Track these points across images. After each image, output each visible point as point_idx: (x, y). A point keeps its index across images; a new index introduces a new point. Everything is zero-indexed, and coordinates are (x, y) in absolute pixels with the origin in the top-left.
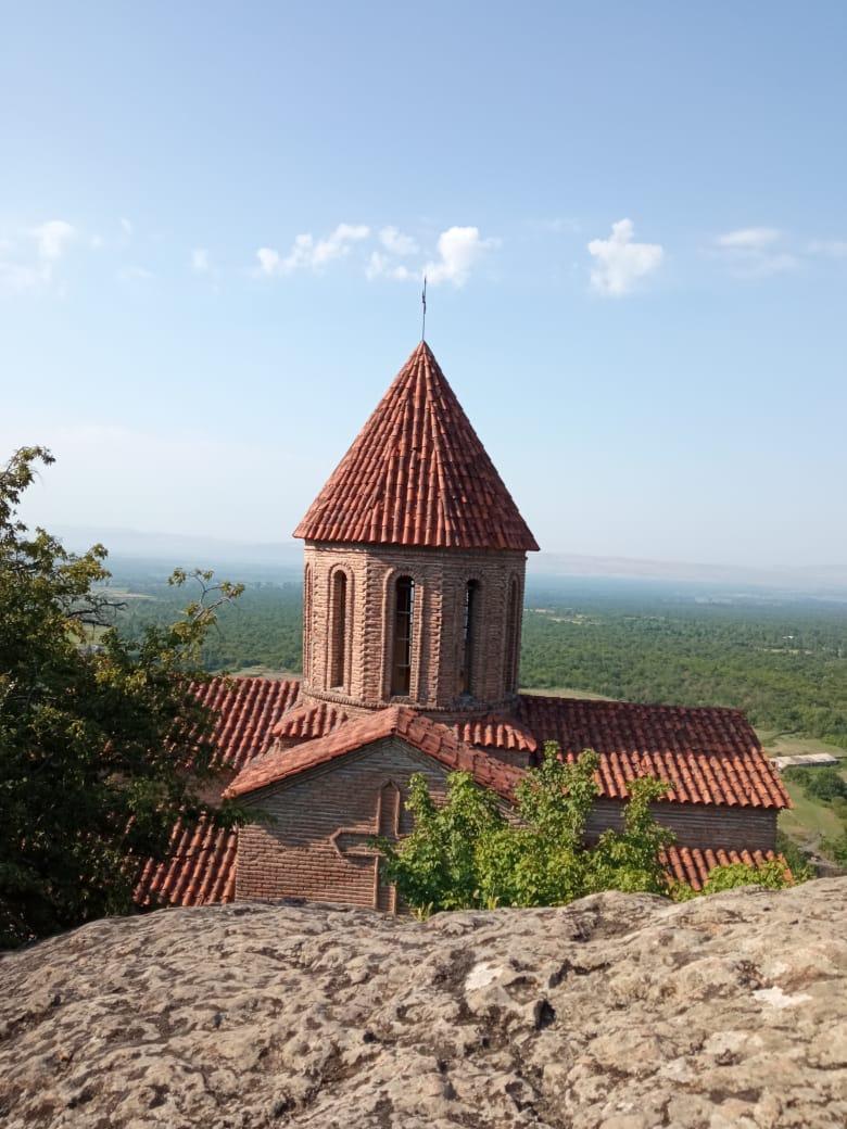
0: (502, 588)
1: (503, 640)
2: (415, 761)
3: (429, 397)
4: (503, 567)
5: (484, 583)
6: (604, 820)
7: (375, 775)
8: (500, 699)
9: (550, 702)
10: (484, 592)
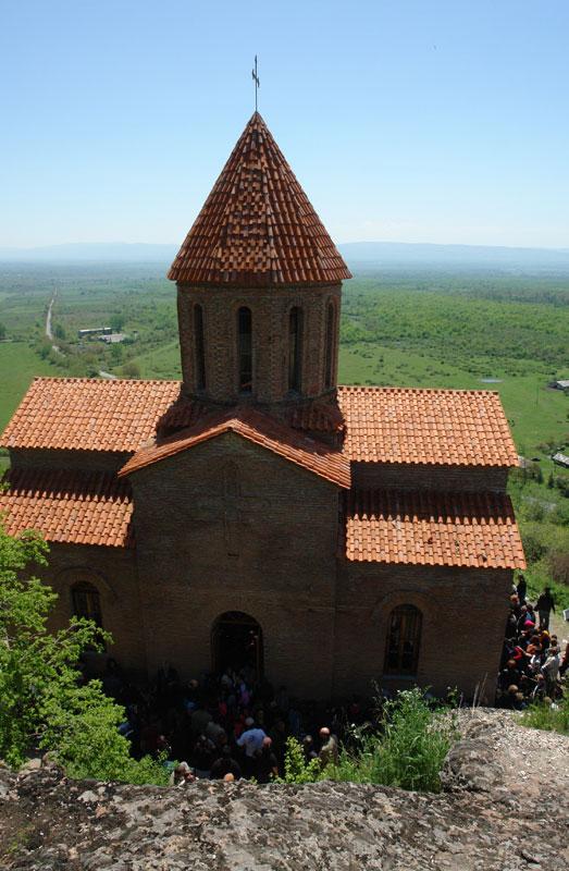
1: (322, 350)
4: (320, 295)
5: (304, 308)
8: (320, 393)
10: (306, 316)
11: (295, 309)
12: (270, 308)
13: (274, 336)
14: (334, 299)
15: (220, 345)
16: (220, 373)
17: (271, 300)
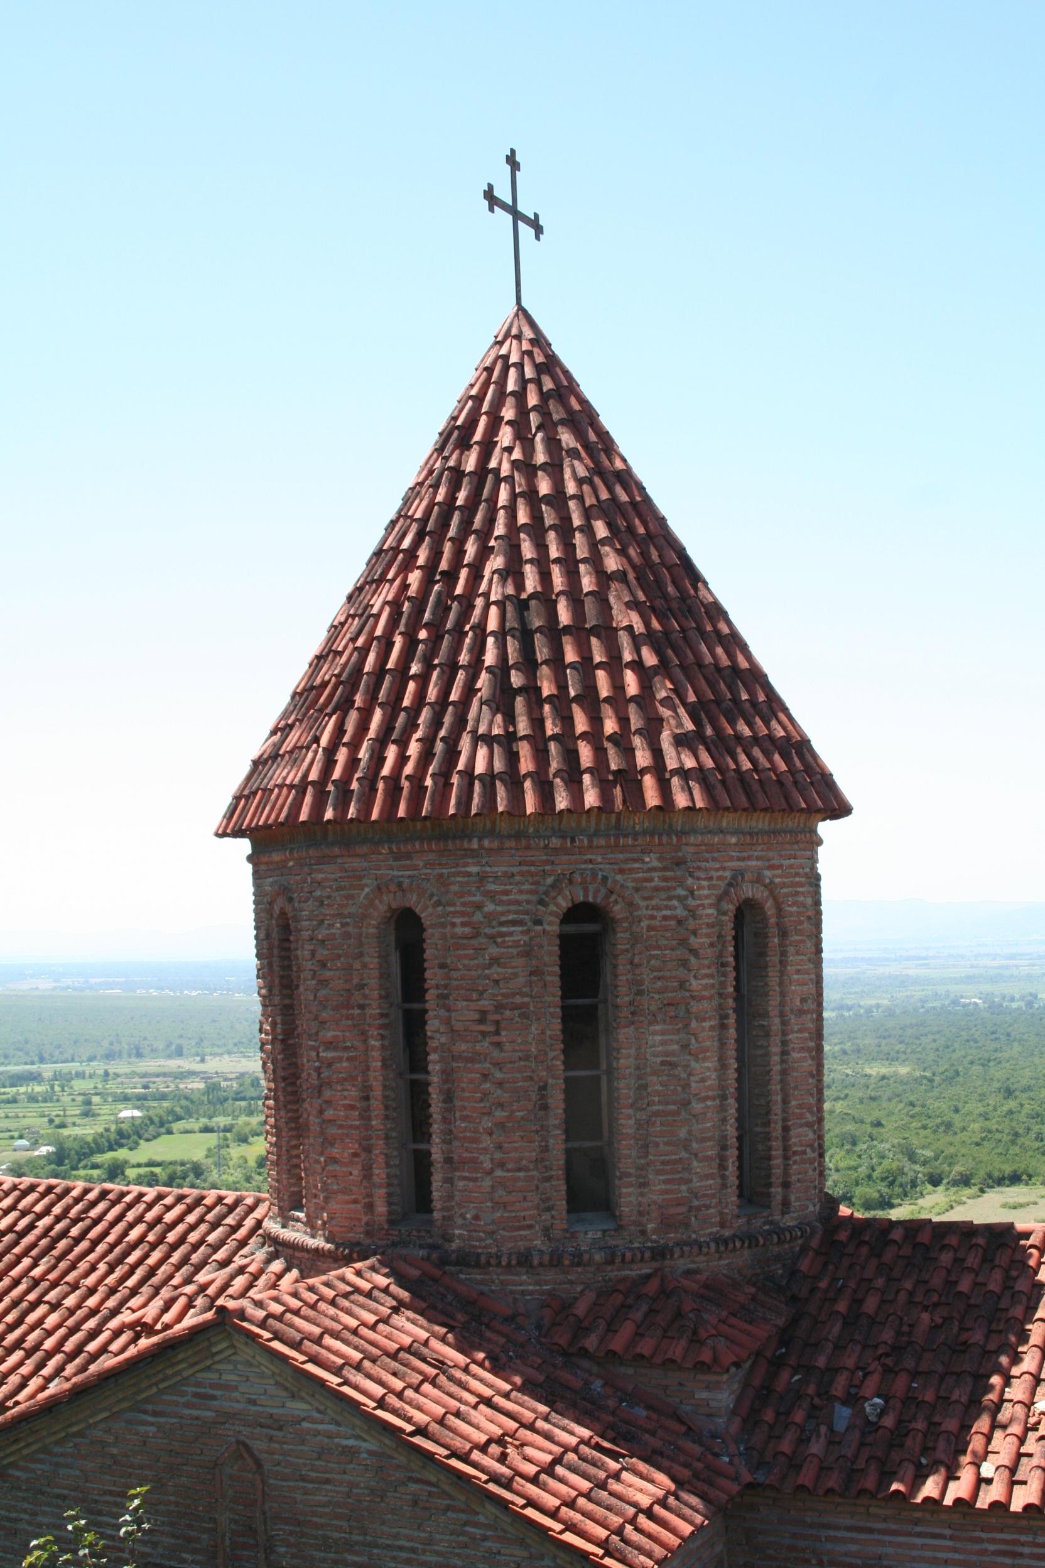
0: (680, 922)
3: (505, 436)
4: (679, 863)
5: (618, 910)
9: (896, 1235)
11: (580, 912)
12: (479, 907)
13: (499, 1007)
14: (771, 887)
15: (330, 1045)
17: (482, 878)
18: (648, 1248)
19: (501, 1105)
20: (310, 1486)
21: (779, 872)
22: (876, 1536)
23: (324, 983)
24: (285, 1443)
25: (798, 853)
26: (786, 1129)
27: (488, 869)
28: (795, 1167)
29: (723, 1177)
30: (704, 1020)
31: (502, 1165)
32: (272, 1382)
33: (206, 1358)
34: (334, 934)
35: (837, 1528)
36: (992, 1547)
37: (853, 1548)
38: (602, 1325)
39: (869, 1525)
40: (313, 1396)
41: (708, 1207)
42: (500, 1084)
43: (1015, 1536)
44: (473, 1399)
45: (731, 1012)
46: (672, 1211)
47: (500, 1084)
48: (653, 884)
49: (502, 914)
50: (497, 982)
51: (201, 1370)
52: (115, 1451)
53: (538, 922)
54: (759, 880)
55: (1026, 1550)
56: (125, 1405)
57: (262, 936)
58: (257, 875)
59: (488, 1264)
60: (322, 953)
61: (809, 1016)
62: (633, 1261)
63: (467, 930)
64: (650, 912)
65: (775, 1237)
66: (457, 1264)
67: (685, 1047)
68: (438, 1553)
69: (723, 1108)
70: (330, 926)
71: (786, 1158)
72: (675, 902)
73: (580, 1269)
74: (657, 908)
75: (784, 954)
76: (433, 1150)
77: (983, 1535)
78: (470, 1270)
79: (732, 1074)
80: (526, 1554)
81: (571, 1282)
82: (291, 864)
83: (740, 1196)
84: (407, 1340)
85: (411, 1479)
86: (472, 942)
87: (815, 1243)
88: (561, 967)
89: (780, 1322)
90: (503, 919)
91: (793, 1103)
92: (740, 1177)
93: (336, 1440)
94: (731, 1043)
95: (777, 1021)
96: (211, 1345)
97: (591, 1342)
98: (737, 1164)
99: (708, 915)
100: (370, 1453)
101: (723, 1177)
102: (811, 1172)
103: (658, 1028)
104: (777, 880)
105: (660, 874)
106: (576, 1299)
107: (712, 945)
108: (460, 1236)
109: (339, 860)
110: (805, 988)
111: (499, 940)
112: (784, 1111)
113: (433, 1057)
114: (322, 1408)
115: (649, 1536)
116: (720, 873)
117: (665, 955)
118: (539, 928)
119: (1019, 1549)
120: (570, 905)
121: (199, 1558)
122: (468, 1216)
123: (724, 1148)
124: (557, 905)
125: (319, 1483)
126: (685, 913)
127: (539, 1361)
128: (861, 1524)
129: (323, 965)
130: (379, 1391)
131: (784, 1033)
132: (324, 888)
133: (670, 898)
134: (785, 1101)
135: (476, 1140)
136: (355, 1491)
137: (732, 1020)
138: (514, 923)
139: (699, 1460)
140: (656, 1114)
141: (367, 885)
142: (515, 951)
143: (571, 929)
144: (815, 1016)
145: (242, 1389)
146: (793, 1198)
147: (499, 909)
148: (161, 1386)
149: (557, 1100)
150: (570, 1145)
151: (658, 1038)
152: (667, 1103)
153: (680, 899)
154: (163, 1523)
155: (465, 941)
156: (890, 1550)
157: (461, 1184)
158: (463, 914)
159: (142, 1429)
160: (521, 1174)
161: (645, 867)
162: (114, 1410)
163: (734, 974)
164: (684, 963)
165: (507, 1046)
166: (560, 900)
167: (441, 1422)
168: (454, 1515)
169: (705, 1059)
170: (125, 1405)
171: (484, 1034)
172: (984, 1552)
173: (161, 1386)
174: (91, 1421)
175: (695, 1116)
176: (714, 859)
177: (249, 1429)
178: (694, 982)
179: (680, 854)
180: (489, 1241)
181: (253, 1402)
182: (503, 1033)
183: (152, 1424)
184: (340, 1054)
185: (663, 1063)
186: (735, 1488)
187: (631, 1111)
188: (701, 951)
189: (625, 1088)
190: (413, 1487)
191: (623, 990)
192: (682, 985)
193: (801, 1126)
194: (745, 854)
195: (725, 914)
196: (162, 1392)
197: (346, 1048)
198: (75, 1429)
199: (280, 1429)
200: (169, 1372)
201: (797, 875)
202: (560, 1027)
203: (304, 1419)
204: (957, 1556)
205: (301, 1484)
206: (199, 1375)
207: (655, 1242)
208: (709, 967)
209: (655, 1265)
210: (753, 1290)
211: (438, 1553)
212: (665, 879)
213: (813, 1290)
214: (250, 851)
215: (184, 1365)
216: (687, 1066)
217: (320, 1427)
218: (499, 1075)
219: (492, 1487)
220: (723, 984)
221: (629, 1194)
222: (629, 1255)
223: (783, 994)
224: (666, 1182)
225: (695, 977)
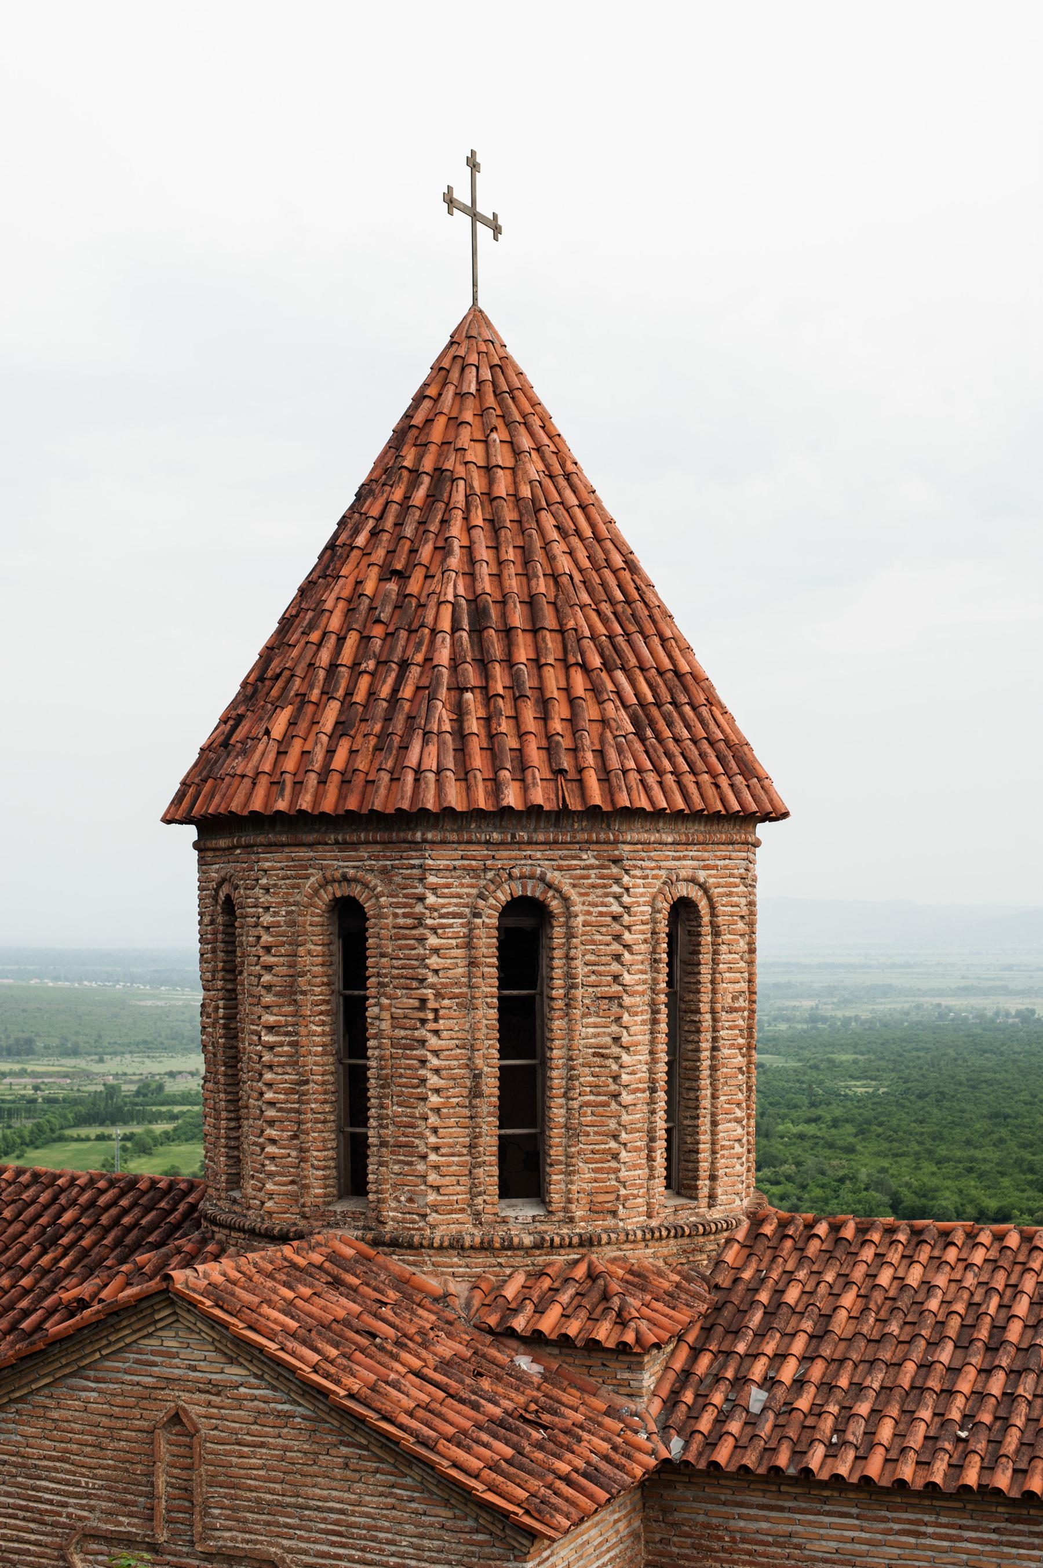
0: (616, 918)
2: (231, 1361)
5: (555, 905)
6: (834, 1545)
7: (148, 1395)
8: (633, 1220)
12: (421, 899)
14: (703, 887)
15: (270, 1029)
16: (271, 1123)
18: (577, 1234)
19: (437, 1091)
20: (246, 1449)
21: (714, 872)
22: (787, 1515)
23: (269, 968)
24: (222, 1408)
25: (734, 854)
26: (714, 1123)
27: (430, 862)
28: (723, 1161)
29: (652, 1169)
30: (636, 1014)
31: (436, 1149)
32: (212, 1348)
33: (149, 1325)
34: (279, 922)
35: (750, 1506)
36: (896, 1527)
37: (764, 1525)
38: (529, 1308)
39: (780, 1503)
40: (251, 1361)
41: (636, 1197)
42: (437, 1071)
43: (919, 1516)
44: (403, 1370)
45: (663, 1007)
46: (601, 1198)
47: (437, 1071)
48: (590, 881)
49: (443, 906)
50: (436, 972)
51: (144, 1337)
52: (55, 1415)
53: (476, 915)
54: (693, 880)
55: (930, 1530)
56: (67, 1371)
57: (207, 919)
58: (202, 862)
59: (422, 1246)
60: (266, 939)
61: (740, 1013)
62: (561, 1246)
63: (409, 921)
64: (586, 908)
65: (701, 1228)
66: (389, 1245)
67: (616, 1040)
68: (367, 1515)
69: (652, 1102)
70: (276, 914)
71: (714, 1152)
72: (611, 900)
73: (509, 1253)
74: (595, 905)
75: (716, 952)
76: (371, 1133)
77: (889, 1514)
78: (403, 1251)
79: (662, 1067)
80: (450, 1514)
81: (500, 1265)
82: (238, 851)
83: (667, 1187)
84: (341, 1314)
85: (342, 1443)
86: (414, 932)
87: (740, 1235)
88: (499, 958)
89: (703, 1308)
90: (444, 910)
91: (722, 1098)
92: (668, 1169)
93: (272, 1405)
94: (662, 1038)
95: (708, 1016)
96: (155, 1311)
97: (519, 1323)
98: (665, 1155)
99: (642, 913)
100: (304, 1418)
101: (652, 1169)
102: (738, 1167)
103: (592, 1020)
104: (712, 880)
105: (596, 871)
106: (505, 1281)
107: (645, 941)
108: (393, 1219)
109: (287, 849)
110: (737, 986)
111: (440, 931)
112: (713, 1105)
113: (371, 1043)
114: (260, 1373)
115: (567, 1500)
116: (655, 872)
117: (600, 950)
118: (478, 921)
119: (923, 1529)
120: (509, 899)
121: (136, 1520)
122: (403, 1199)
123: (652, 1140)
124: (496, 899)
125: (254, 1446)
126: (621, 909)
127: (468, 1338)
128: (773, 1502)
129: (268, 949)
130: (316, 1358)
131: (715, 1030)
132: (271, 876)
133: (607, 895)
134: (714, 1097)
135: (413, 1126)
136: (288, 1454)
137: (663, 1017)
138: (455, 916)
139: (619, 1435)
140: (587, 1104)
141: (312, 874)
142: (454, 942)
143: (511, 922)
144: (746, 1013)
145: (181, 1356)
146: (719, 1191)
147: (441, 901)
148: (104, 1352)
149: (491, 1085)
150: (503, 1132)
151: (591, 1030)
152: (599, 1094)
153: (618, 897)
154: (102, 1487)
155: (407, 932)
156: (799, 1528)
157: (396, 1168)
158: (405, 905)
159: (84, 1394)
160: (455, 1159)
161: (582, 863)
162: (57, 1376)
163: (667, 970)
164: (618, 958)
165: (445, 1034)
166: (499, 894)
167: (373, 1389)
168: (383, 1477)
169: (636, 1053)
170: (67, 1371)
171: (423, 1021)
172: (888, 1532)
173: (104, 1352)
174: (34, 1387)
175: (625, 1107)
176: (650, 859)
177: (188, 1395)
178: (626, 976)
179: (616, 852)
180: (421, 1224)
181: (194, 1369)
182: (441, 1022)
183: (93, 1390)
184: (282, 1038)
185: (595, 1055)
186: (652, 1462)
187: (562, 1101)
188: (635, 947)
189: (557, 1077)
190: (344, 1450)
191: (558, 983)
192: (616, 978)
193: (729, 1121)
194: (681, 854)
195: (659, 912)
196: (104, 1357)
197: (288, 1034)
198: (17, 1395)
199: (218, 1394)
200: (112, 1338)
201: (731, 876)
202: (496, 1016)
203: (241, 1385)
204: (864, 1535)
205: (237, 1447)
206: (141, 1342)
207: (583, 1228)
208: (642, 963)
209: (583, 1250)
210: (677, 1278)
211: (367, 1515)
212: (602, 877)
213: (736, 1280)
214: (195, 837)
215: (127, 1332)
216: (617, 1058)
217: (257, 1392)
218: (435, 1062)
219: (419, 1449)
220: (655, 982)
221: (558, 1182)
222: (557, 1240)
223: (714, 991)
224: (594, 1171)
225: (628, 971)
